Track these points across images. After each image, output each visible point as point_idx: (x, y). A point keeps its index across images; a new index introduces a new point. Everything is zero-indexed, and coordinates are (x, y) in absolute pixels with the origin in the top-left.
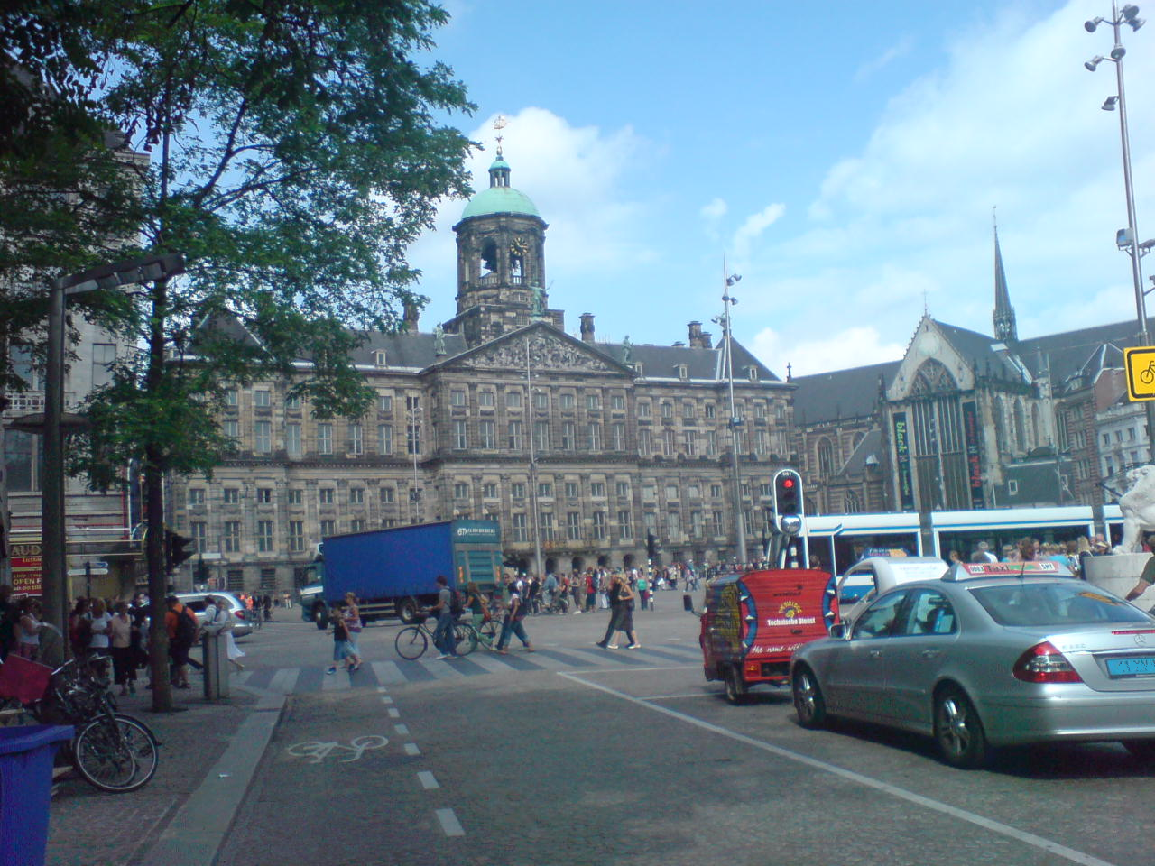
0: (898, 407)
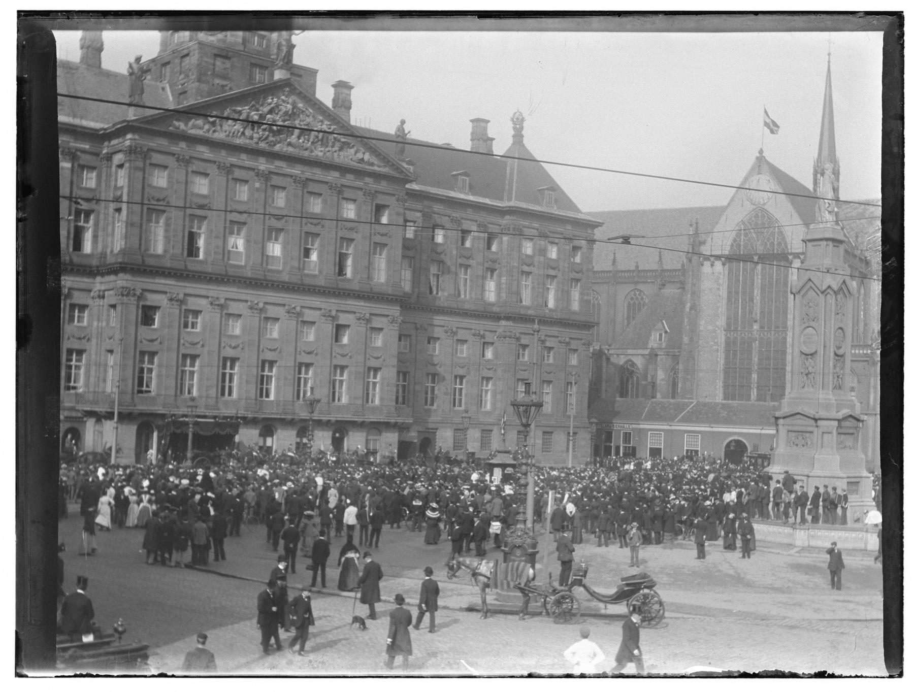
0: (712, 265)
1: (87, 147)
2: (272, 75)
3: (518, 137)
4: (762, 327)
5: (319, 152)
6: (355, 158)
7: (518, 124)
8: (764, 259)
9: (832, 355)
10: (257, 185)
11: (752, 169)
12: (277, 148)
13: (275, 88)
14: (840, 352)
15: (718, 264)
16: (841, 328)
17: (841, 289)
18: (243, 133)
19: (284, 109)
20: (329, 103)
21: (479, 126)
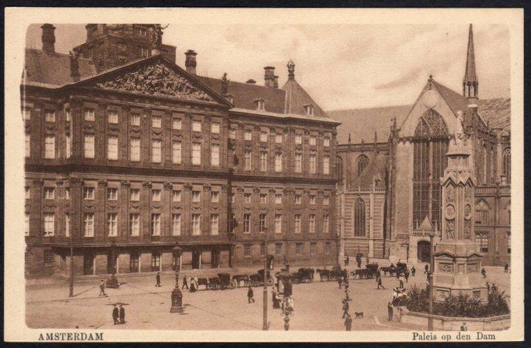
0: (404, 143)
1: (49, 99)
2: (150, 52)
3: (291, 76)
4: (434, 178)
5: (178, 95)
6: (199, 97)
7: (291, 68)
8: (435, 140)
9: (463, 221)
10: (145, 116)
11: (425, 88)
12: (156, 94)
13: (152, 61)
14: (468, 218)
15: (407, 143)
16: (468, 205)
17: (468, 183)
18: (136, 87)
19: (158, 72)
20: (185, 68)
21: (269, 72)
